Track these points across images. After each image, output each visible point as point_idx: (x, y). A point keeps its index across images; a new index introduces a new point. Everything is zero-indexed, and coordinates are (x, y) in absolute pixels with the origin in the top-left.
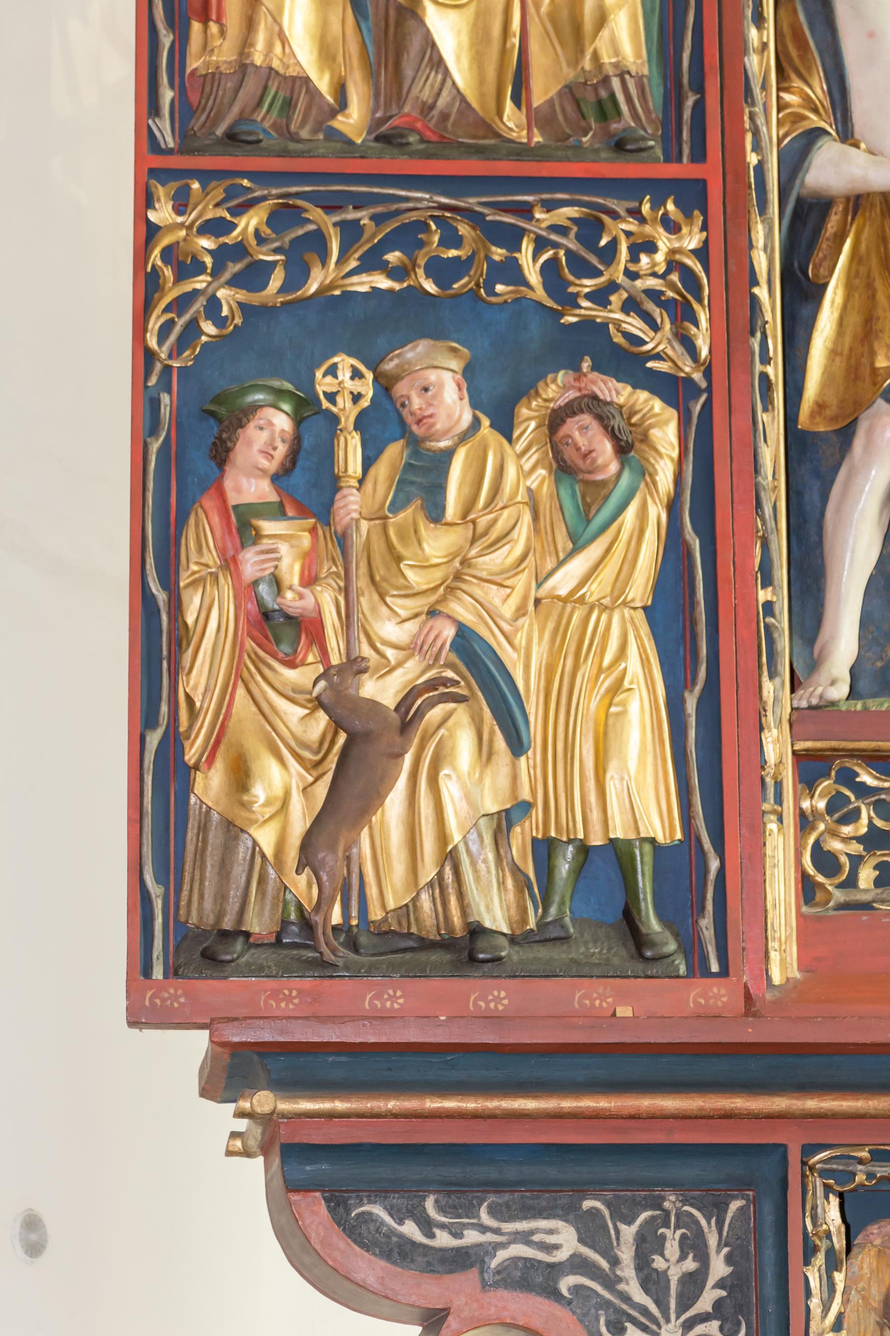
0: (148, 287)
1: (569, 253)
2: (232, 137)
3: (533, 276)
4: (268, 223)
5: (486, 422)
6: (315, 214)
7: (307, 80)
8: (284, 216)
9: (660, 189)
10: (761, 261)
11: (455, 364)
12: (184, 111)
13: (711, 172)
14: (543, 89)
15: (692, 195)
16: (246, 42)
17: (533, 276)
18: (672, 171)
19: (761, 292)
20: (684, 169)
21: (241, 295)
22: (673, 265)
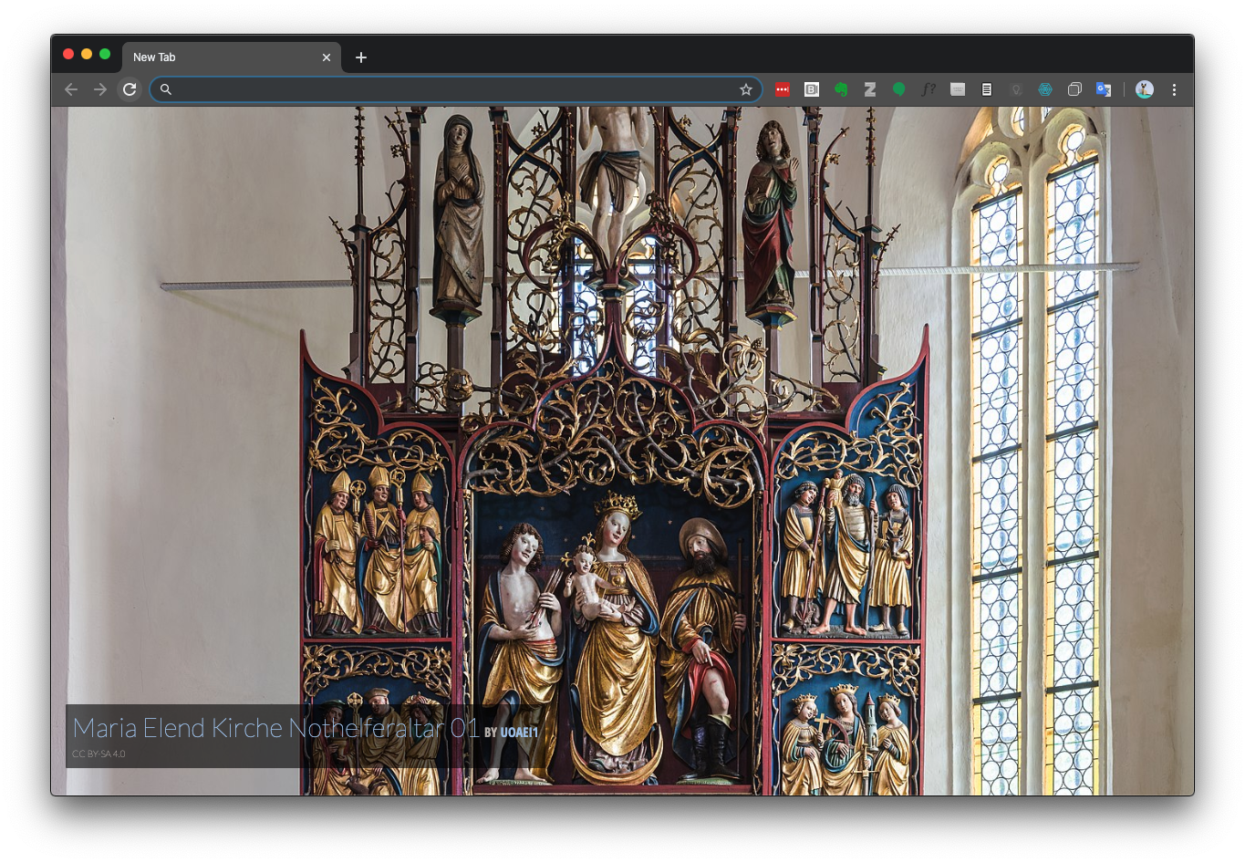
0: (304, 675)
1: (415, 663)
2: (325, 633)
3: (406, 671)
4: (336, 657)
5: (393, 710)
6: (348, 654)
7: (346, 616)
8: (340, 655)
9: (439, 645)
10: (467, 664)
11: (386, 695)
12: (314, 625)
13: (453, 640)
14: (409, 617)
15: (448, 646)
16: (329, 607)
17: (406, 671)
18: (443, 640)
19: (466, 673)
20: (446, 639)
21: (328, 677)
22: (443, 665)
